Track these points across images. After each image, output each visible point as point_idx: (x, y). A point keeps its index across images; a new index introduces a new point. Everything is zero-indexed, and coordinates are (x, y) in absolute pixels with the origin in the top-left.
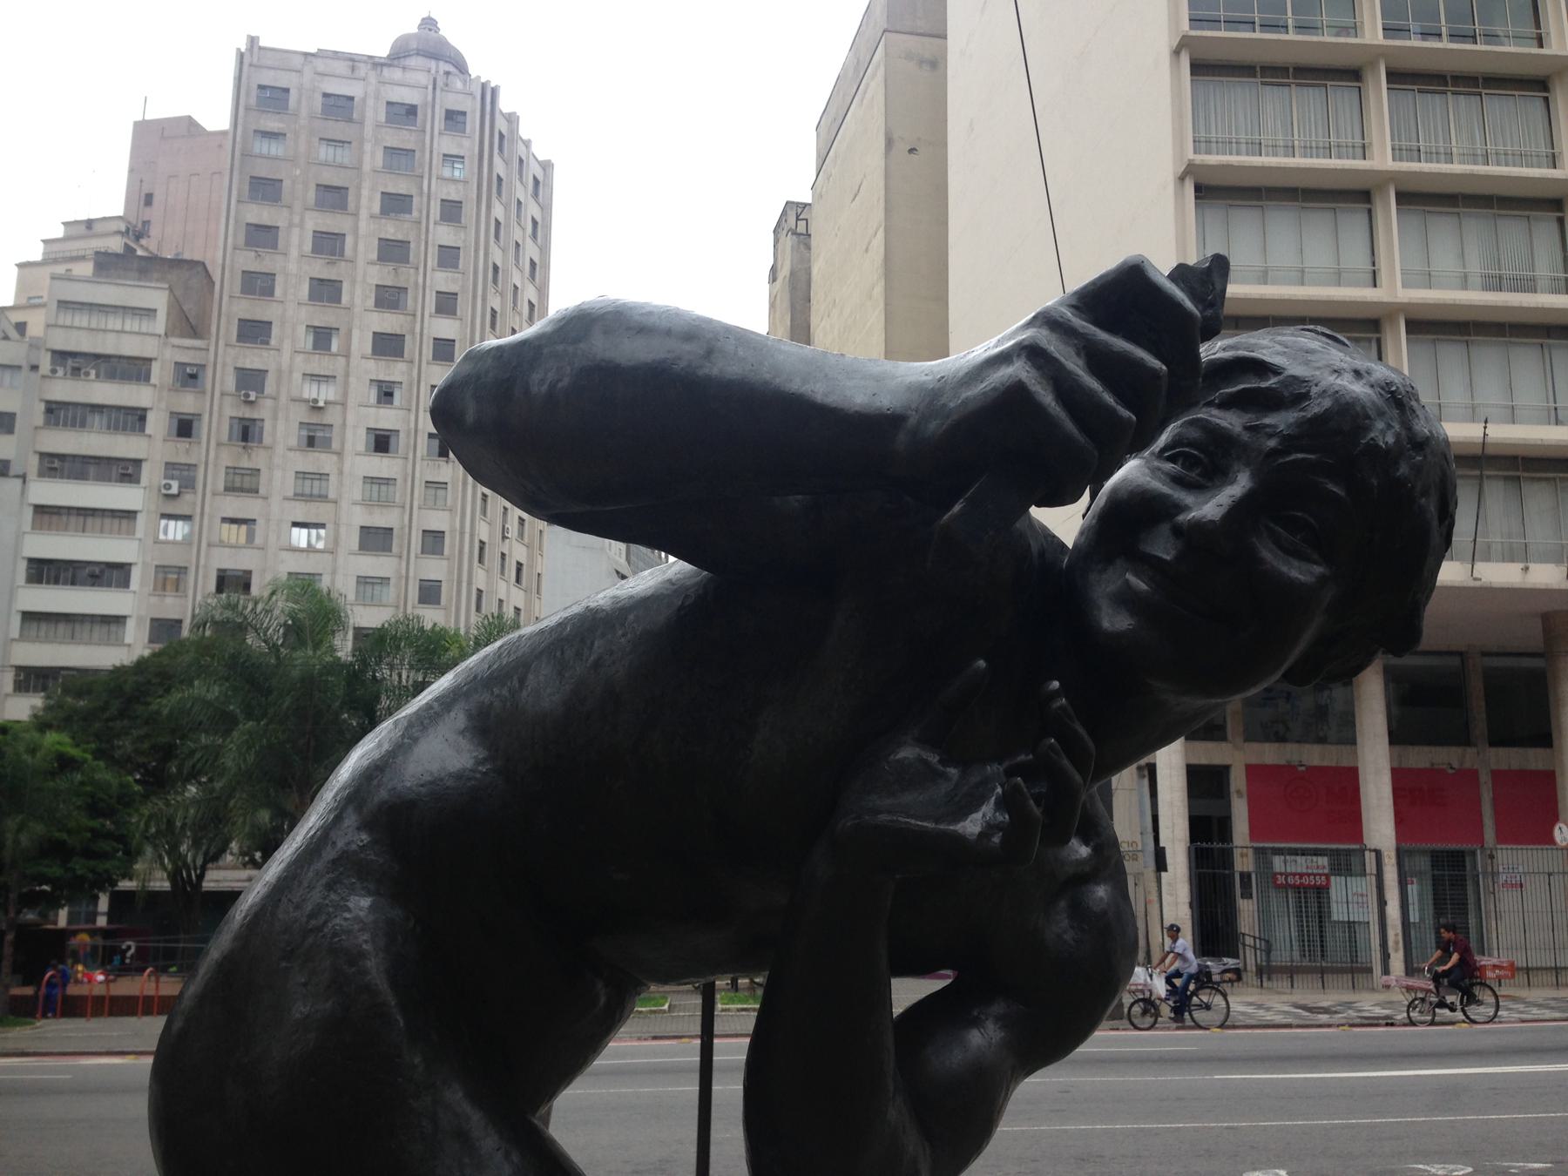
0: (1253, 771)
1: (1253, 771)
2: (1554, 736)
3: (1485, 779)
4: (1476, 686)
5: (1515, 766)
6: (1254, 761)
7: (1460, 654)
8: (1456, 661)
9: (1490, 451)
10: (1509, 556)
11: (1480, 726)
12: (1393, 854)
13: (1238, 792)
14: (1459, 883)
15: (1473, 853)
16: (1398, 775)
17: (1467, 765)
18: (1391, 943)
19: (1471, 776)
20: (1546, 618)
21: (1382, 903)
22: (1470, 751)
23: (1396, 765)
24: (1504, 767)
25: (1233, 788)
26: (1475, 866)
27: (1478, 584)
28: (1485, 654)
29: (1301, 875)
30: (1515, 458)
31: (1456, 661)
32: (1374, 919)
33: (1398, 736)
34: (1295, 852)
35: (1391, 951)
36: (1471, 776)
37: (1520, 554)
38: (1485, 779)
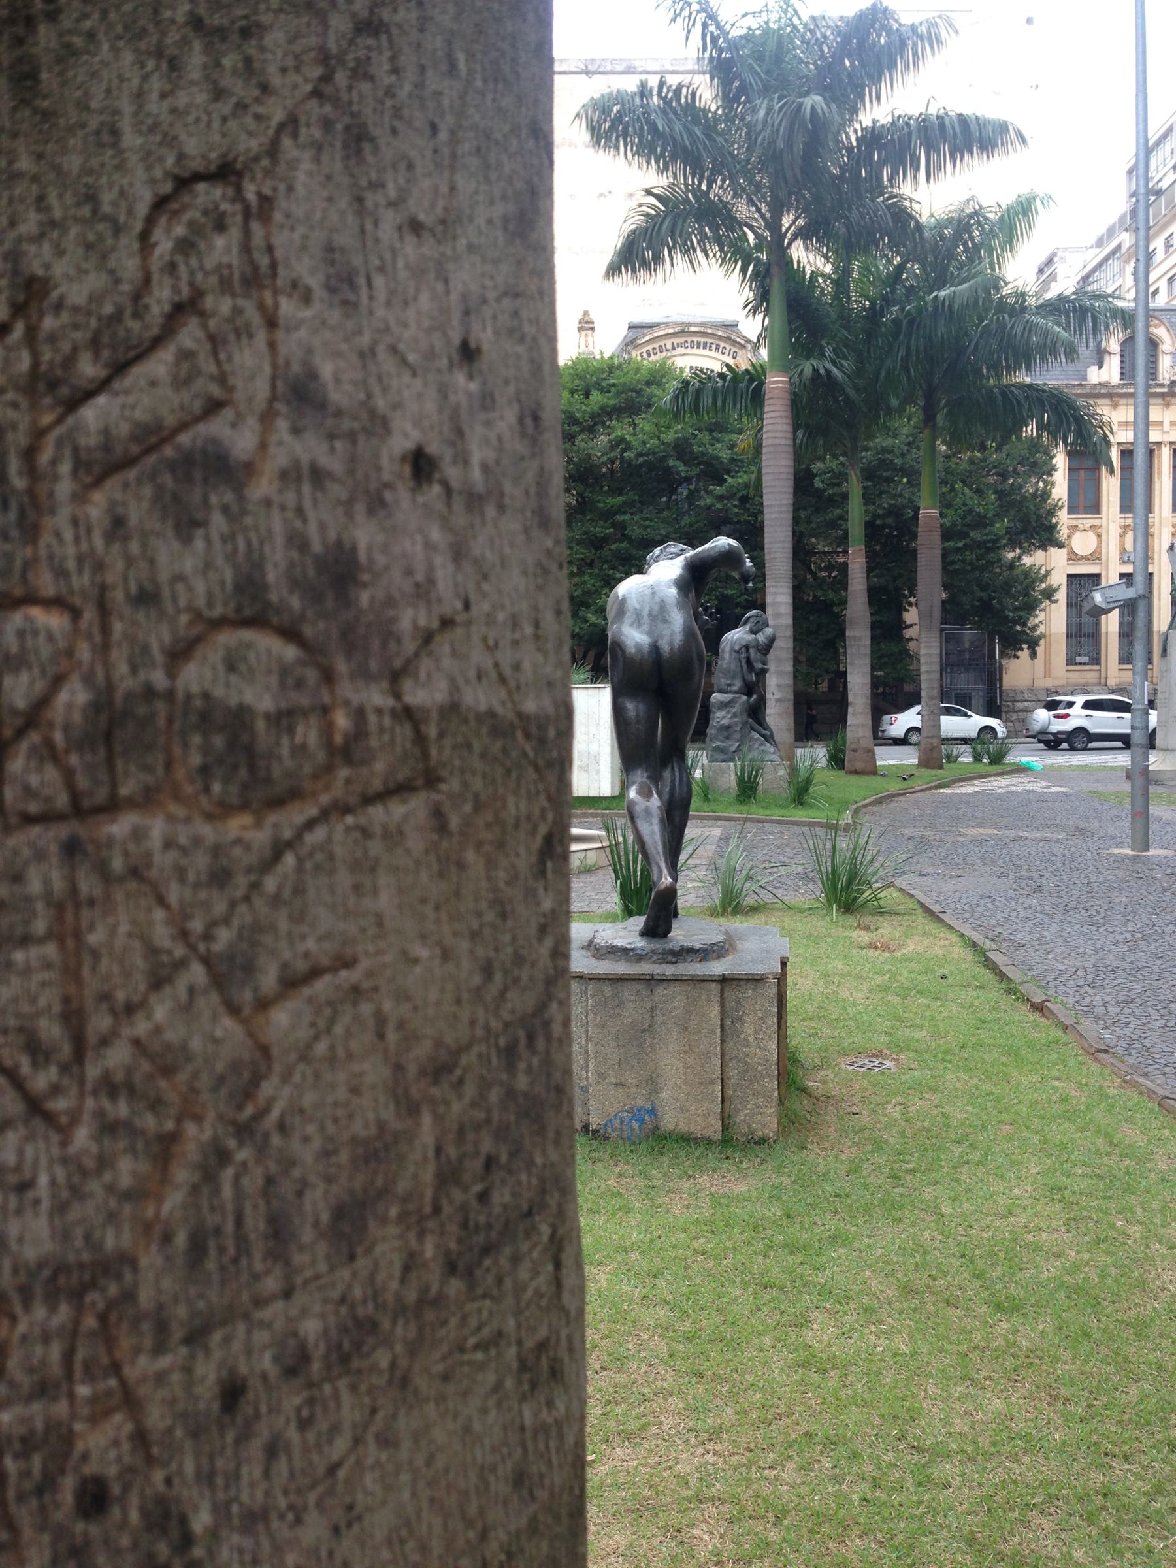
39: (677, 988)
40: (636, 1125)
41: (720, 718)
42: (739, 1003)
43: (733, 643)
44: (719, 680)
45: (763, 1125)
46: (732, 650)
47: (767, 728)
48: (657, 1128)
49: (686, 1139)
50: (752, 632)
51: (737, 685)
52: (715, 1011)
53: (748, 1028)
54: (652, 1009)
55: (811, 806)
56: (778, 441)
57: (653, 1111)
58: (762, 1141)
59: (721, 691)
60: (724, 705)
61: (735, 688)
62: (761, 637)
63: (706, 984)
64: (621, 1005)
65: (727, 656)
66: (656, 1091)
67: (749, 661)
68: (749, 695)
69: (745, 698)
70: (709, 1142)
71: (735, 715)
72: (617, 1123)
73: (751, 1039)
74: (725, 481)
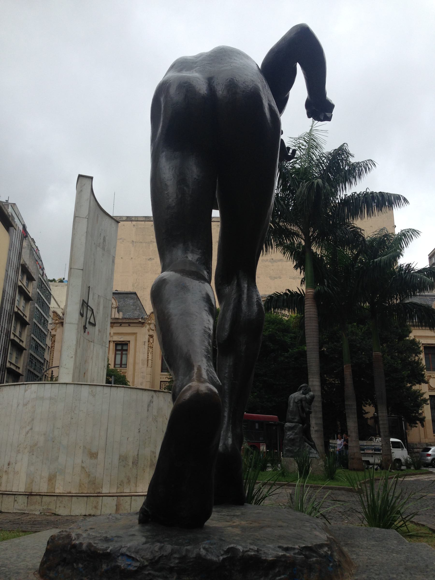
41: (289, 435)
43: (295, 398)
44: (289, 417)
46: (294, 402)
47: (312, 441)
50: (303, 393)
51: (297, 419)
55: (337, 480)
56: (311, 313)
59: (290, 422)
60: (291, 429)
61: (296, 420)
62: (308, 396)
65: (291, 404)
67: (302, 408)
68: (303, 424)
69: (301, 425)
71: (296, 434)
74: (288, 351)
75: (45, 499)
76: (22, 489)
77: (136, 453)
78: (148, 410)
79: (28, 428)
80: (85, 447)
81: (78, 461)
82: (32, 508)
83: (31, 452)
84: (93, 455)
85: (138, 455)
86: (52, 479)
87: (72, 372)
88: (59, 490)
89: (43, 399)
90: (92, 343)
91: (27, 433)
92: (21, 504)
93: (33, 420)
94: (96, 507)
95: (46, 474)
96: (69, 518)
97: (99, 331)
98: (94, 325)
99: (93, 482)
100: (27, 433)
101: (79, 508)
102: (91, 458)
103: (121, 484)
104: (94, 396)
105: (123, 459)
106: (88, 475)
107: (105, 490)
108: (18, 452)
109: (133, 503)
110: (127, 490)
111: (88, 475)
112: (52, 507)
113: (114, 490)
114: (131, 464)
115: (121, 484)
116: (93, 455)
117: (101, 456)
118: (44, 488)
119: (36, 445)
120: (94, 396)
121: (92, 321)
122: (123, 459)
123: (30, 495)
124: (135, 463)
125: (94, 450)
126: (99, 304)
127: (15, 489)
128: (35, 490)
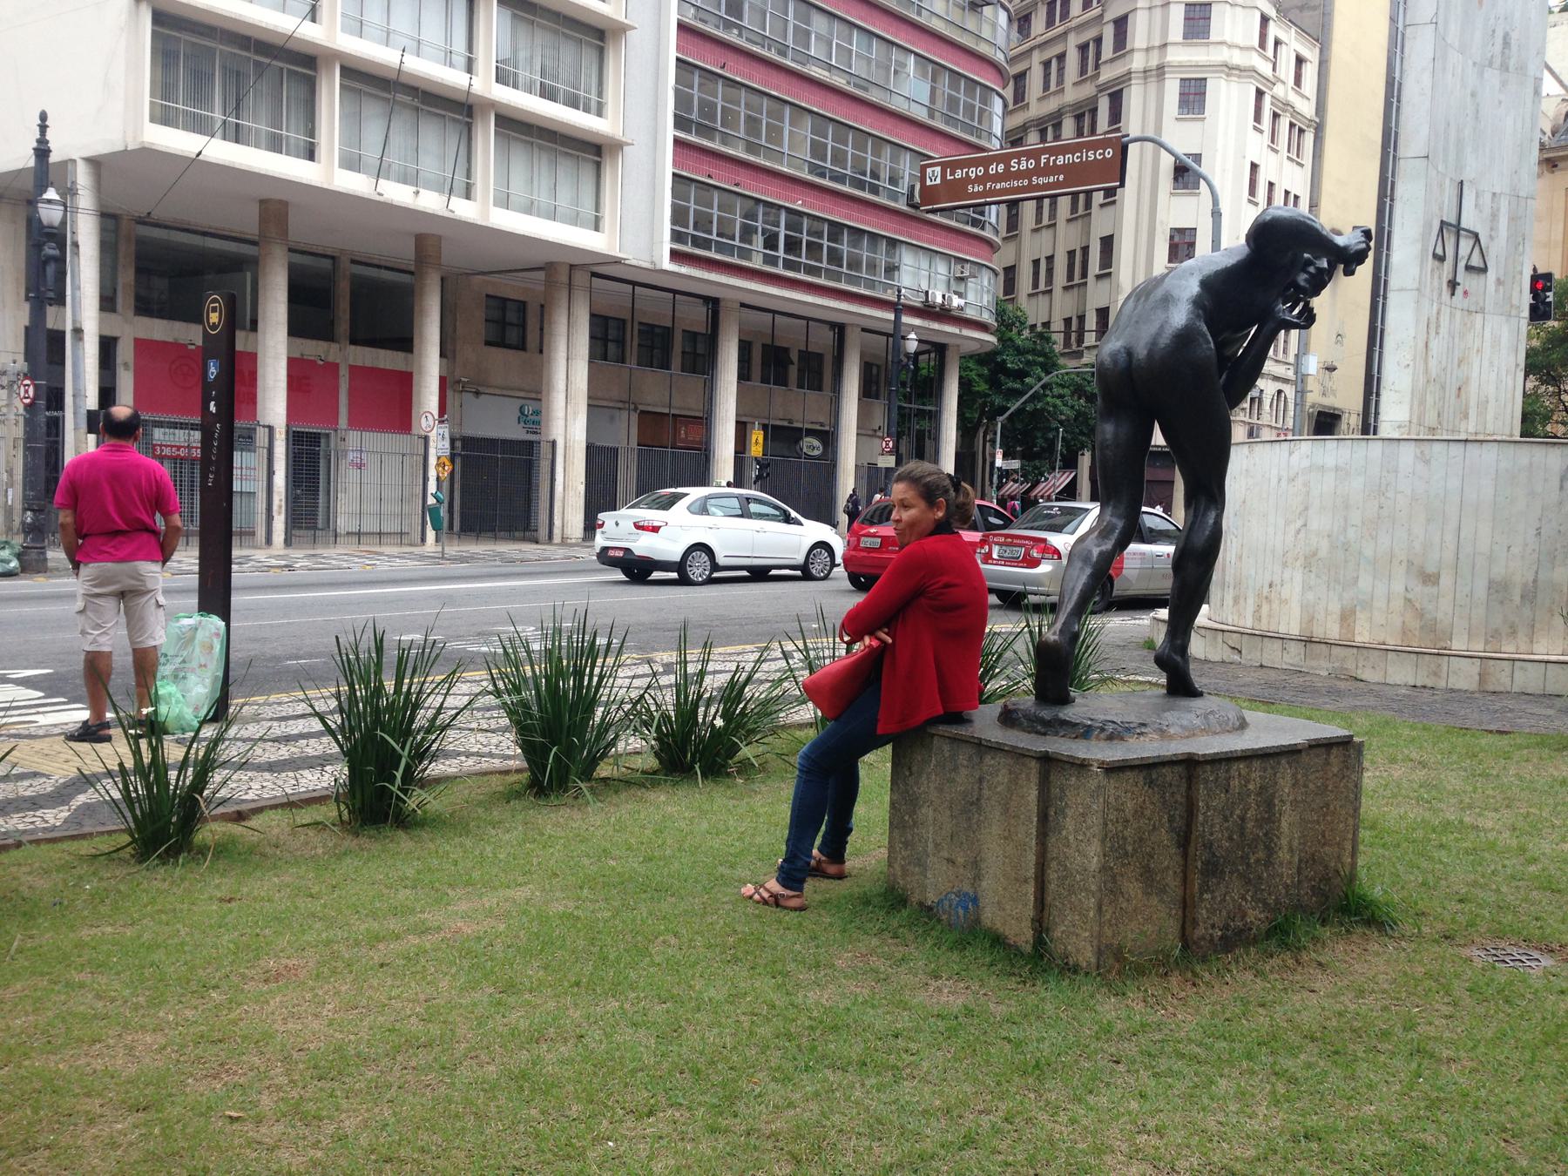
0: (142, 346)
1: (142, 346)
2: (416, 341)
3: (344, 374)
4: (343, 290)
5: (368, 364)
6: (142, 335)
7: (333, 258)
8: (327, 264)
9: (403, 79)
10: (404, 179)
11: (343, 327)
12: (284, 431)
13: (126, 364)
14: (314, 458)
15: (328, 435)
16: (292, 362)
17: (331, 359)
18: (275, 508)
19: (333, 368)
20: (420, 240)
21: (270, 473)
22: (335, 346)
23: (297, 355)
24: (360, 364)
25: (119, 360)
26: (328, 445)
27: (380, 199)
28: (353, 262)
29: (179, 448)
30: (416, 89)
31: (327, 264)
32: (263, 484)
33: (297, 329)
34: (175, 426)
35: (275, 514)
36: (335, 366)
37: (410, 178)
38: (344, 374)
39: (1002, 760)
40: (961, 912)
42: (1062, 790)
45: (1078, 950)
48: (978, 921)
49: (997, 941)
52: (1033, 794)
53: (1069, 824)
54: (981, 780)
57: (975, 900)
58: (1075, 969)
63: (1027, 760)
64: (955, 769)
66: (978, 878)
70: (1019, 953)
72: (946, 903)
73: (1071, 838)
75: (1336, 650)
76: (1295, 631)
77: (1531, 579)
78: (1561, 488)
79: (1299, 523)
80: (1410, 563)
81: (1398, 587)
82: (1314, 663)
83: (1307, 567)
84: (1430, 579)
85: (1535, 581)
86: (1347, 617)
87: (1407, 399)
88: (1362, 637)
89: (1322, 469)
90: (1479, 317)
91: (1298, 531)
92: (1293, 656)
93: (1306, 509)
94: (1435, 674)
95: (1335, 607)
96: (1376, 688)
97: (1499, 282)
98: (1484, 270)
99: (1430, 627)
100: (1298, 531)
101: (1402, 674)
102: (1424, 582)
103: (1495, 635)
104: (1427, 462)
105: (1498, 589)
106: (1420, 614)
107: (1458, 644)
108: (1285, 565)
109: (1517, 674)
110: (1509, 649)
111: (1420, 614)
112: (1350, 665)
113: (1478, 647)
114: (1517, 599)
115: (1495, 635)
116: (1430, 579)
117: (1446, 581)
118: (1333, 631)
119: (1315, 554)
120: (1427, 462)
121: (1476, 261)
122: (1498, 589)
123: (1308, 641)
124: (1530, 595)
125: (1431, 569)
126: (1494, 216)
127: (1283, 629)
128: (1318, 633)
